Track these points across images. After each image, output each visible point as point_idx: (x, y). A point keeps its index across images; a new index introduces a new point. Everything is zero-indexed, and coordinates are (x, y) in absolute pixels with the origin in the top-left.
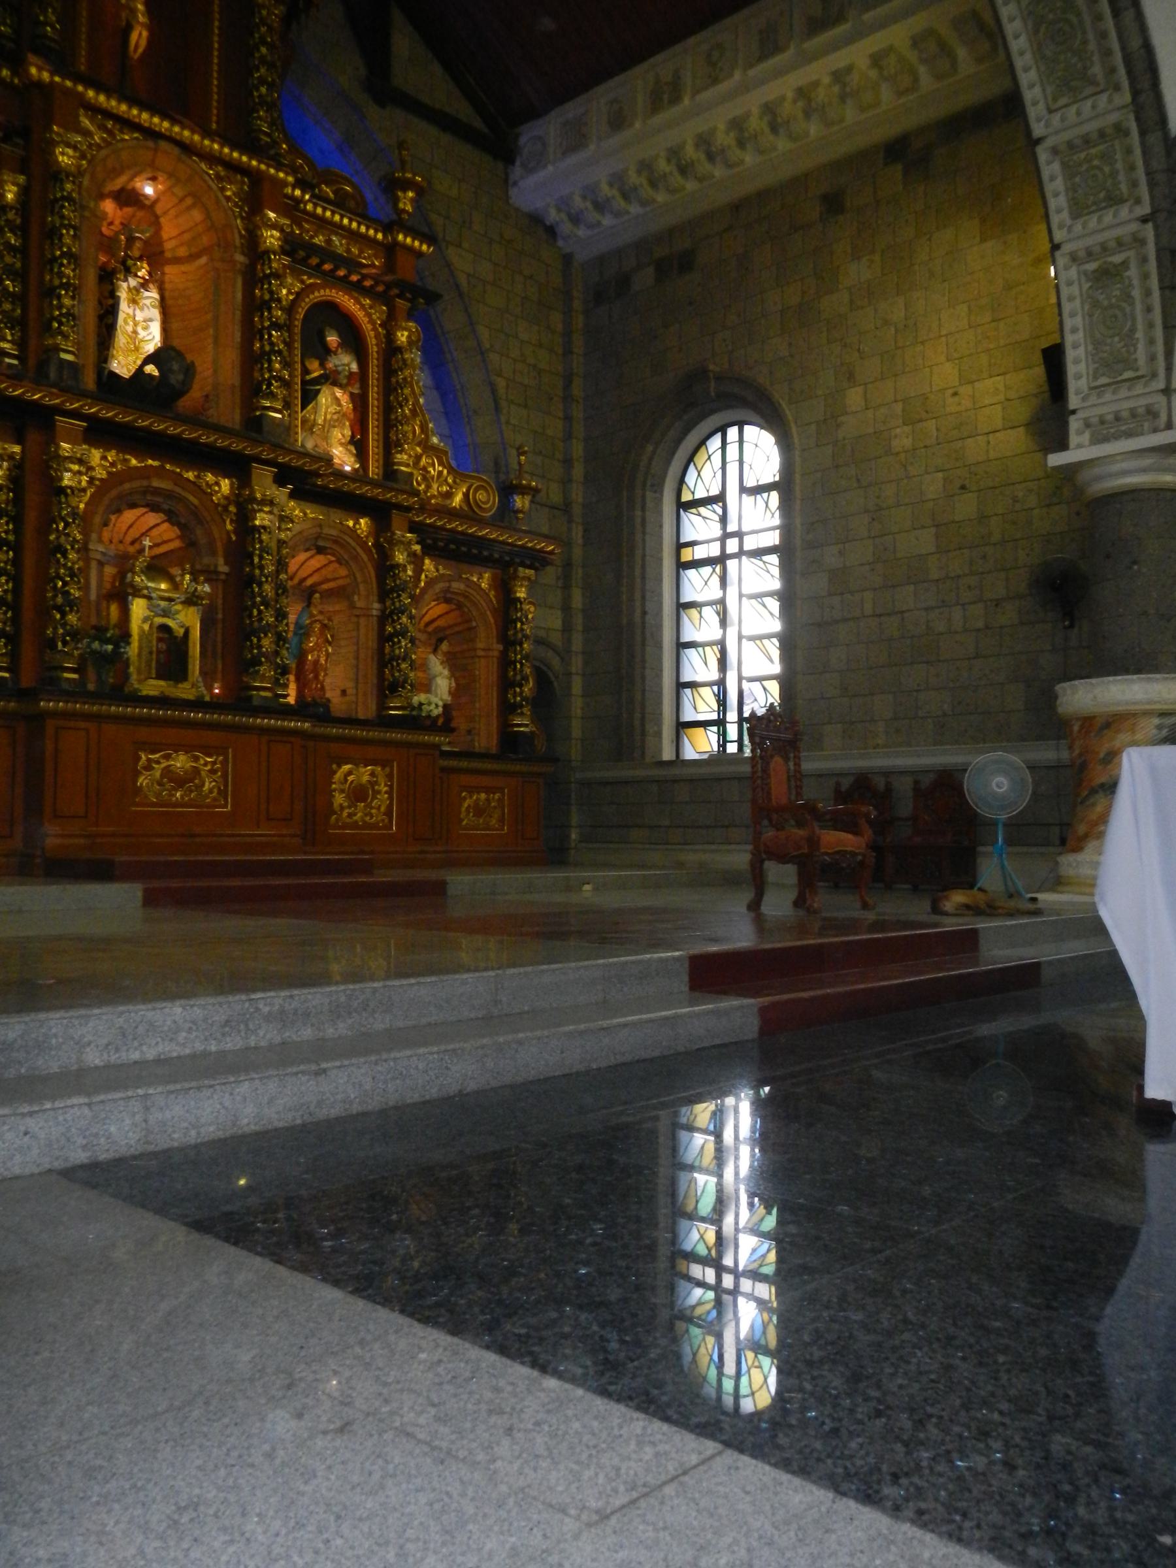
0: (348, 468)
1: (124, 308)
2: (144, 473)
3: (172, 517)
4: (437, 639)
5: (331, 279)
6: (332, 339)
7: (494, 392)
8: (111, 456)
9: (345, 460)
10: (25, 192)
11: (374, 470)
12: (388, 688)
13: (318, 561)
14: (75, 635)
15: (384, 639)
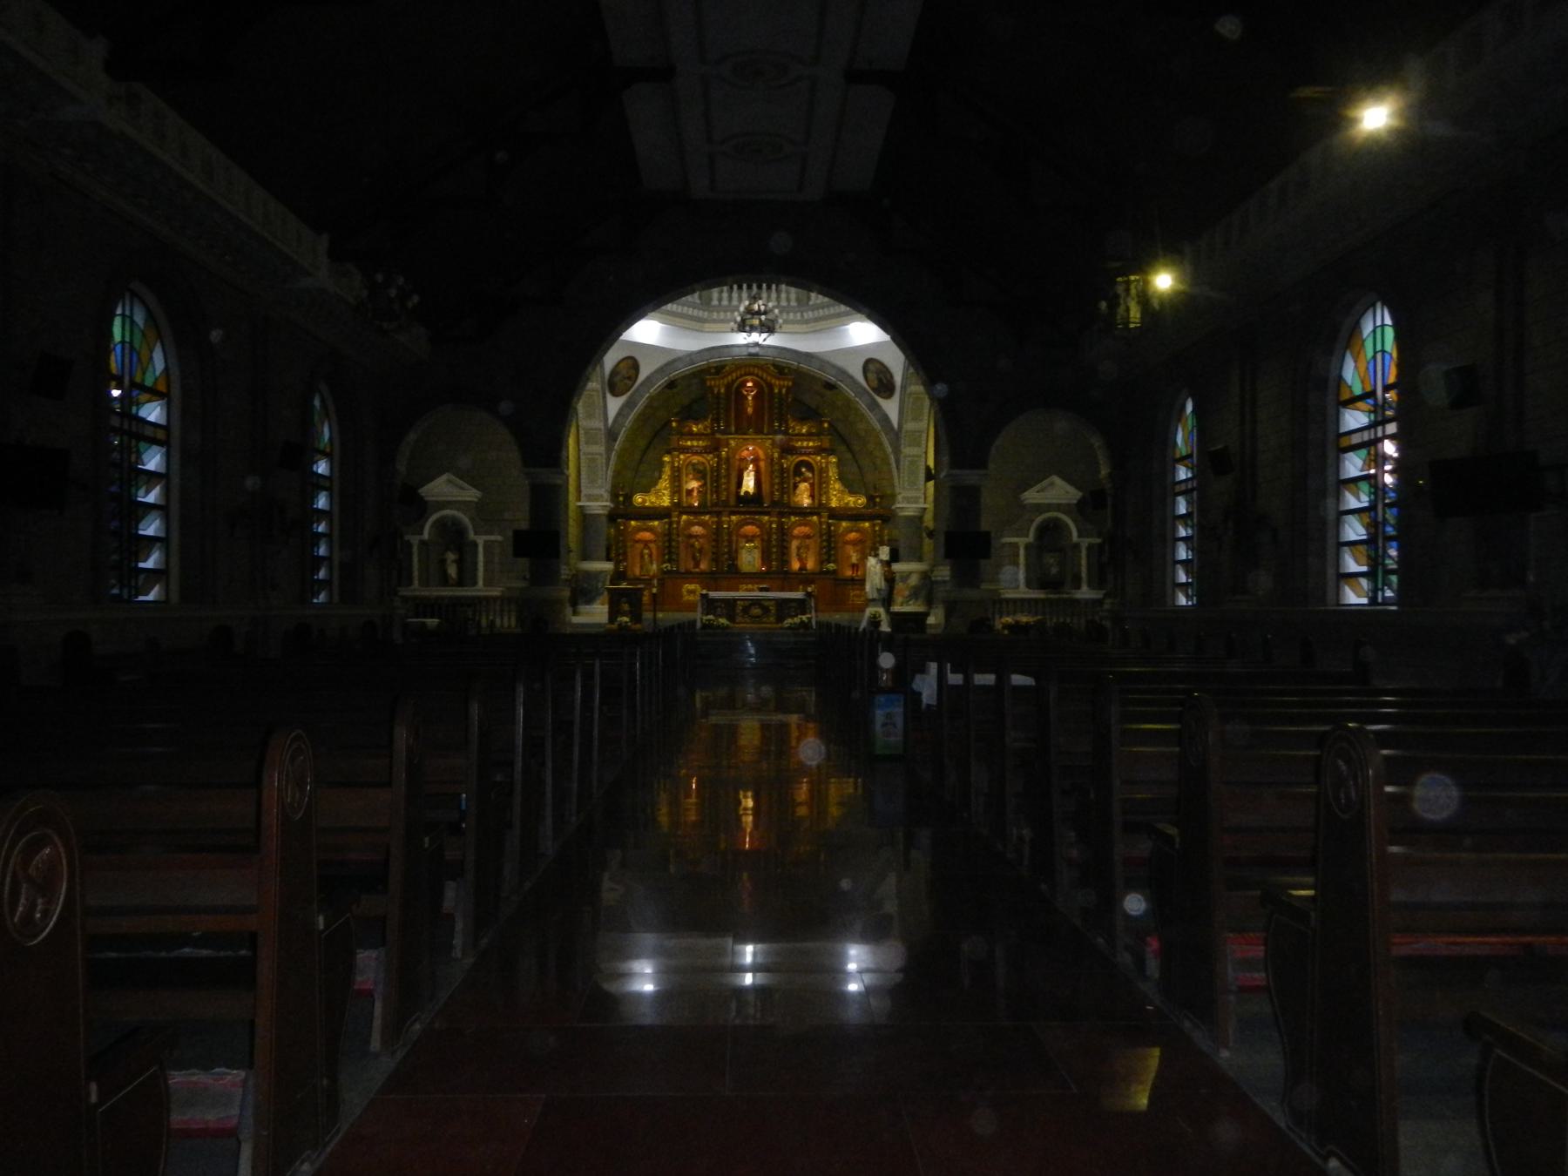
0: (805, 505)
1: (745, 478)
2: (746, 519)
3: (758, 527)
4: (854, 543)
5: (801, 454)
6: (804, 470)
7: (874, 463)
8: (738, 516)
9: (806, 502)
10: (718, 463)
11: (816, 501)
12: (822, 563)
13: (807, 528)
14: (727, 560)
15: (821, 548)
